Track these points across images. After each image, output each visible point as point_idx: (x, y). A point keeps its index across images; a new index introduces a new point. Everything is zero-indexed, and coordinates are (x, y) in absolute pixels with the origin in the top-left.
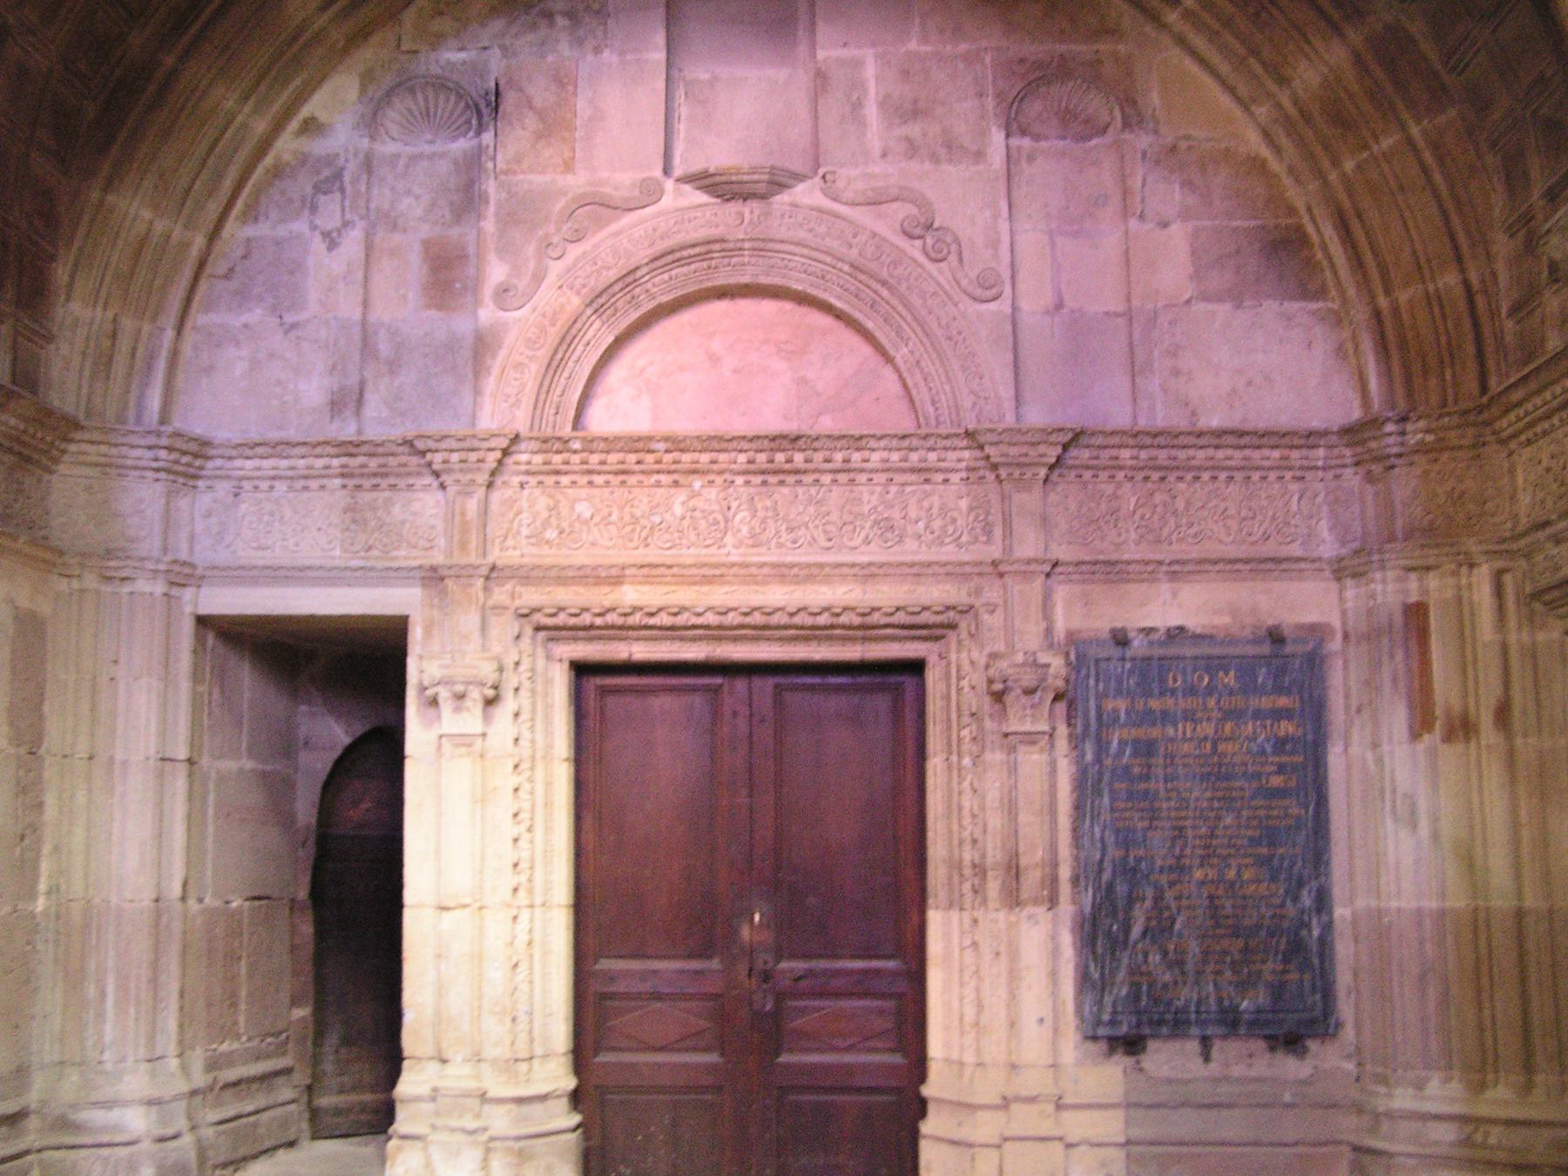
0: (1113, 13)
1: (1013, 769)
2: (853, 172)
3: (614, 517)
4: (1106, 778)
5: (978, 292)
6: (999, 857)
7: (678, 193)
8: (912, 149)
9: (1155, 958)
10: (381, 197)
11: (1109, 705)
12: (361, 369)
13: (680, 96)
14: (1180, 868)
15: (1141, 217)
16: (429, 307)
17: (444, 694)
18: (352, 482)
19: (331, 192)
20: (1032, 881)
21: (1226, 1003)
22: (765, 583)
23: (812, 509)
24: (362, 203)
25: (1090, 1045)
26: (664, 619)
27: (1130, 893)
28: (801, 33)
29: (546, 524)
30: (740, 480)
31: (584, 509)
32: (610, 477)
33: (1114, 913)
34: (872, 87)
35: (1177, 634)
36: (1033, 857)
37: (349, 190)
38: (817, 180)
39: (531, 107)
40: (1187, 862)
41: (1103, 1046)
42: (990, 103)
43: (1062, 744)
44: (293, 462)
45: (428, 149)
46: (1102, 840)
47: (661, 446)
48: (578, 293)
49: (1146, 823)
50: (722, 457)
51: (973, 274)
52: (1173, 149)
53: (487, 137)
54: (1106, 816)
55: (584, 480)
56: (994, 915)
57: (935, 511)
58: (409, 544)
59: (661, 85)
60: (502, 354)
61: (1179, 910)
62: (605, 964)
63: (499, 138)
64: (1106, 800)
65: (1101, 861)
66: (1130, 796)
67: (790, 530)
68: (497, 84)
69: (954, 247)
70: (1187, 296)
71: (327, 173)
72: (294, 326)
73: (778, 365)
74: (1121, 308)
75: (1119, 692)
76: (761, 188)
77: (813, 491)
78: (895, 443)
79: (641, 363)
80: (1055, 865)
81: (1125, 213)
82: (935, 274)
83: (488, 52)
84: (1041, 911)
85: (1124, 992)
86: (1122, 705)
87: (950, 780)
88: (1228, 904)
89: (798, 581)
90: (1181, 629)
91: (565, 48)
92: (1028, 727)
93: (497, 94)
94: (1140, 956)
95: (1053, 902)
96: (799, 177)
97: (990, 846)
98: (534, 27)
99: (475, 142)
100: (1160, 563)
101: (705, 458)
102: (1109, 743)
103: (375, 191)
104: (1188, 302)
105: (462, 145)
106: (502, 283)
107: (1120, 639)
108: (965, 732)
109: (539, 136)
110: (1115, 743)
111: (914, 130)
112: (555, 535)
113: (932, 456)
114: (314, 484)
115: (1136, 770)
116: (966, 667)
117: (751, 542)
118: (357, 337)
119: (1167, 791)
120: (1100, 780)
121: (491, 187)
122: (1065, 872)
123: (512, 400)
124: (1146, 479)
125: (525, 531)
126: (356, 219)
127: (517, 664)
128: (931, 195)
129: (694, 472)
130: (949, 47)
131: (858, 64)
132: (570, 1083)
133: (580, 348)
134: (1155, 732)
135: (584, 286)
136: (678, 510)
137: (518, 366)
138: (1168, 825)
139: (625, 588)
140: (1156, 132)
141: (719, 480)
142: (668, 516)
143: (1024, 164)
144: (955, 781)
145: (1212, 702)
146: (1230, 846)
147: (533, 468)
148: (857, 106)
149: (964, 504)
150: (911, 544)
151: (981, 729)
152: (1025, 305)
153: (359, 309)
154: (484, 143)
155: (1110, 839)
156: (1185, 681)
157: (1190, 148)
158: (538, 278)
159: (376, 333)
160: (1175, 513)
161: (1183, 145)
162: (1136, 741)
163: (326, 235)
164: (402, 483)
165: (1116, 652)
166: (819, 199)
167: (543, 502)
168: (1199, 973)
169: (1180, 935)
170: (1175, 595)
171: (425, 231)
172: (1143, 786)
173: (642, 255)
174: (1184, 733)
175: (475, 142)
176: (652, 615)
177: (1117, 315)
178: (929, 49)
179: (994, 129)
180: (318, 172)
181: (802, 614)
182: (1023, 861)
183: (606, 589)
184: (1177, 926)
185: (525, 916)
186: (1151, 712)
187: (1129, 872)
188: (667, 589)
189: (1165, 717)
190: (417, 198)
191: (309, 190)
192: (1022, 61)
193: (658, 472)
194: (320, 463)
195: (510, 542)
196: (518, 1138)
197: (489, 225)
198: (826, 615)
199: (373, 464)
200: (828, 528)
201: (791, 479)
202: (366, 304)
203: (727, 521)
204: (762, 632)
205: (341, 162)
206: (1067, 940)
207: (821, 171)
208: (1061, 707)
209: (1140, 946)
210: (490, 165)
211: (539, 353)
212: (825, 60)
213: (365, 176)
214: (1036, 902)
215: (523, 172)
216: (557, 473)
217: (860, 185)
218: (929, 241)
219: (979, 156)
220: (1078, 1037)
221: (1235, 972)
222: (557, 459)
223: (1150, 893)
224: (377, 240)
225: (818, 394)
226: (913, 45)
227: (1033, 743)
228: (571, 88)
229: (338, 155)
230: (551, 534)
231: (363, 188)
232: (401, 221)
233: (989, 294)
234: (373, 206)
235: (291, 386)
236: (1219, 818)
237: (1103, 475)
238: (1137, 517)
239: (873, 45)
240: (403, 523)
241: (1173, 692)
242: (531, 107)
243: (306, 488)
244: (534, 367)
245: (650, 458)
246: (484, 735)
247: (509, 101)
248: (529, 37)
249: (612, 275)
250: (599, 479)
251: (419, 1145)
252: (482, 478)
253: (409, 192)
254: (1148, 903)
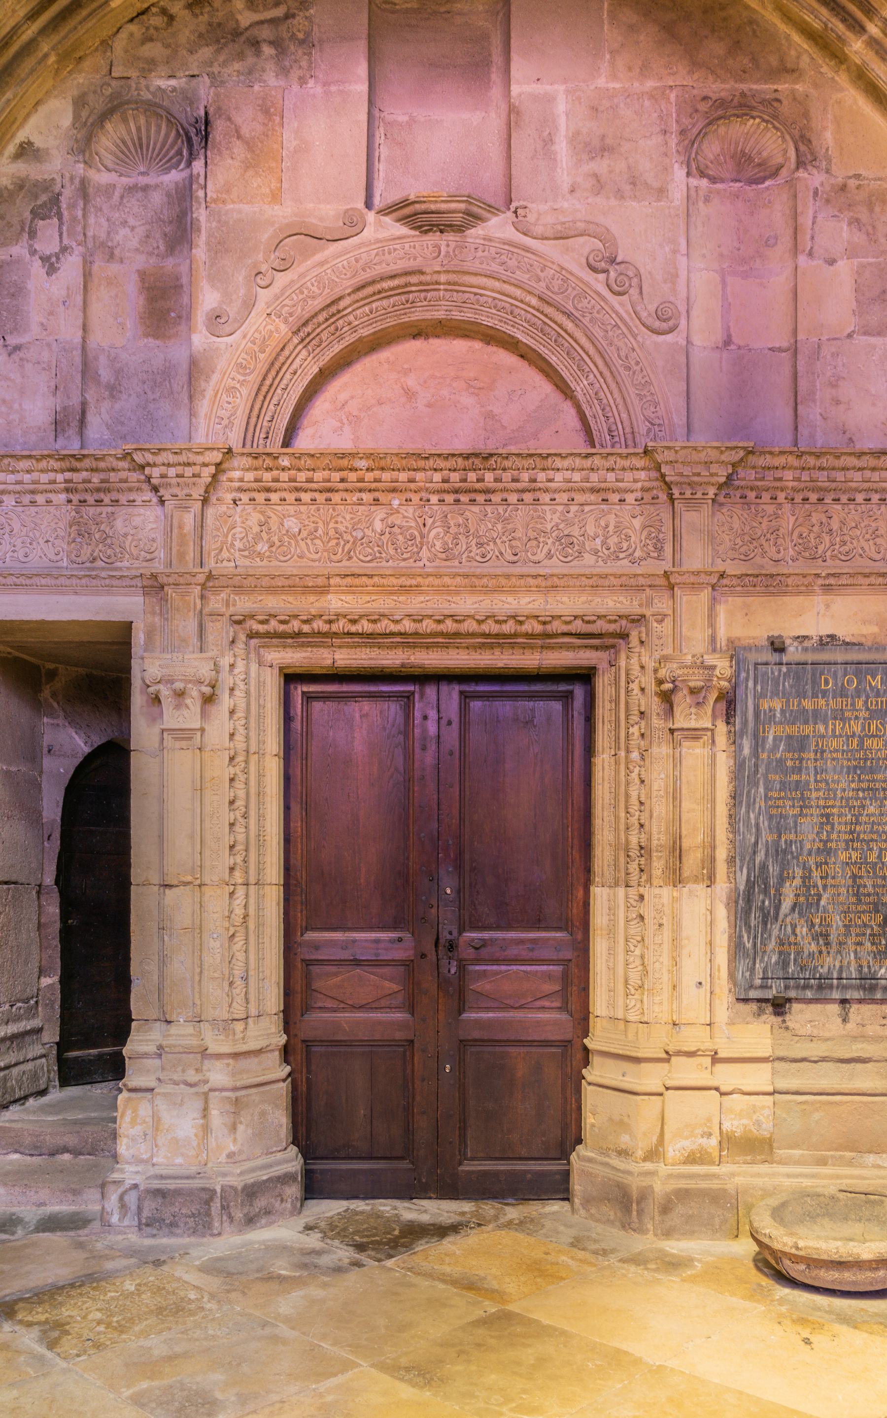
0: (793, 53)
1: (677, 762)
2: (543, 207)
3: (320, 532)
4: (762, 770)
5: (657, 324)
6: (663, 837)
7: (380, 225)
8: (599, 185)
9: (802, 930)
10: (97, 226)
11: (765, 705)
12: (83, 391)
13: (380, 134)
14: (827, 851)
15: (810, 254)
16: (147, 335)
17: (165, 692)
18: (75, 498)
19: (50, 218)
20: (692, 862)
21: (866, 970)
22: (457, 593)
23: (499, 526)
24: (79, 228)
25: (741, 1006)
26: (365, 626)
27: (782, 872)
28: (495, 76)
29: (258, 538)
30: (434, 499)
31: (292, 524)
32: (317, 495)
33: (766, 891)
34: (562, 121)
35: (829, 641)
36: (693, 840)
37: (66, 214)
38: (510, 214)
39: (239, 137)
40: (833, 845)
42: (673, 141)
43: (722, 740)
44: (18, 476)
45: (143, 180)
46: (757, 825)
47: (363, 464)
48: (286, 321)
49: (797, 811)
50: (419, 476)
51: (652, 308)
52: (844, 188)
53: (198, 166)
54: (760, 803)
55: (291, 497)
56: (657, 891)
57: (611, 528)
58: (131, 554)
59: (364, 117)
60: (215, 377)
61: (825, 887)
62: (312, 936)
63: (209, 168)
64: (761, 790)
65: (757, 843)
66: (783, 786)
67: (480, 545)
68: (206, 114)
69: (635, 281)
70: (849, 330)
71: (44, 198)
72: (17, 348)
73: (467, 400)
74: (785, 344)
75: (775, 694)
76: (457, 218)
77: (501, 509)
78: (578, 462)
79: (343, 397)
80: (713, 848)
81: (795, 250)
82: (617, 307)
83: (195, 80)
84: (700, 889)
85: (774, 959)
86: (778, 705)
87: (617, 772)
88: (869, 883)
89: (488, 591)
90: (832, 637)
91: (272, 79)
92: (693, 724)
93: (207, 123)
94: (789, 929)
95: (711, 880)
96: (493, 209)
97: (655, 830)
98: (241, 56)
99: (185, 174)
100: (817, 576)
101: (403, 476)
102: (765, 739)
103: (92, 220)
104: (850, 336)
105: (175, 176)
106: (213, 309)
107: (777, 646)
108: (634, 730)
109: (248, 166)
110: (771, 738)
111: (601, 166)
112: (266, 548)
113: (611, 476)
114: (40, 499)
115: (789, 763)
116: (636, 670)
117: (443, 556)
118: (78, 360)
119: (816, 781)
120: (756, 772)
121: (201, 214)
122: (722, 854)
123: (225, 422)
124: (806, 499)
125: (238, 544)
126: (74, 244)
127: (232, 666)
128: (614, 229)
129: (394, 490)
130: (636, 84)
131: (550, 99)
132: (284, 1039)
133: (288, 376)
134: (808, 730)
135: (291, 315)
136: (378, 526)
137: (231, 390)
138: (815, 812)
139: (330, 597)
140: (828, 171)
141: (415, 498)
142: (369, 532)
143: (701, 204)
144: (623, 773)
145: (860, 704)
146: (872, 832)
147: (245, 485)
148: (549, 141)
149: (637, 523)
150: (589, 559)
151: (649, 726)
152: (697, 340)
153: (80, 333)
154: (195, 172)
155: (764, 824)
156: (835, 684)
157: (858, 187)
158: (249, 304)
159: (96, 359)
161: (852, 183)
162: (790, 737)
163: (45, 259)
164: (123, 499)
165: (775, 657)
166: (510, 233)
167: (255, 518)
169: (825, 910)
170: (828, 606)
171: (140, 261)
172: (795, 777)
173: (348, 284)
174: (834, 730)
175: (188, 171)
176: (354, 622)
177: (781, 350)
178: (617, 85)
179: (676, 166)
180: (36, 197)
181: (489, 621)
182: (686, 844)
183: (312, 598)
184: (822, 903)
185: (241, 892)
186: (804, 711)
187: (780, 853)
188: (368, 598)
189: (817, 716)
190: (133, 228)
191: (27, 215)
192: (705, 98)
193: (360, 491)
194: (45, 478)
195: (225, 554)
196: (235, 1089)
197: (200, 252)
198: (511, 622)
199: (96, 479)
200: (514, 543)
201: (481, 498)
202: (85, 328)
203: (422, 536)
204: (451, 640)
205: (57, 188)
206: (722, 913)
207: (513, 207)
208: (722, 706)
209: (788, 919)
210: (201, 194)
211: (249, 378)
212: (520, 95)
213: (81, 203)
214: (696, 880)
215: (233, 202)
216: (268, 490)
217: (550, 219)
218: (613, 274)
219: (662, 192)
220: (732, 999)
221: (873, 944)
222: (267, 476)
223: (799, 872)
224: (96, 267)
225: (504, 428)
226: (601, 82)
227: (697, 738)
228: (277, 119)
229: (53, 179)
230: (262, 547)
231: (80, 213)
232: (117, 252)
233: (665, 326)
234: (90, 234)
235: (16, 406)
236: (863, 807)
238: (796, 534)
239: (565, 81)
240: (125, 535)
241: (825, 693)
242: (239, 137)
243: (33, 503)
244: (245, 391)
245: (353, 476)
246: (202, 730)
247: (219, 127)
248: (237, 66)
249: (318, 303)
250: (306, 497)
251: (148, 1095)
252: (197, 492)
253: (124, 223)
254: (797, 882)
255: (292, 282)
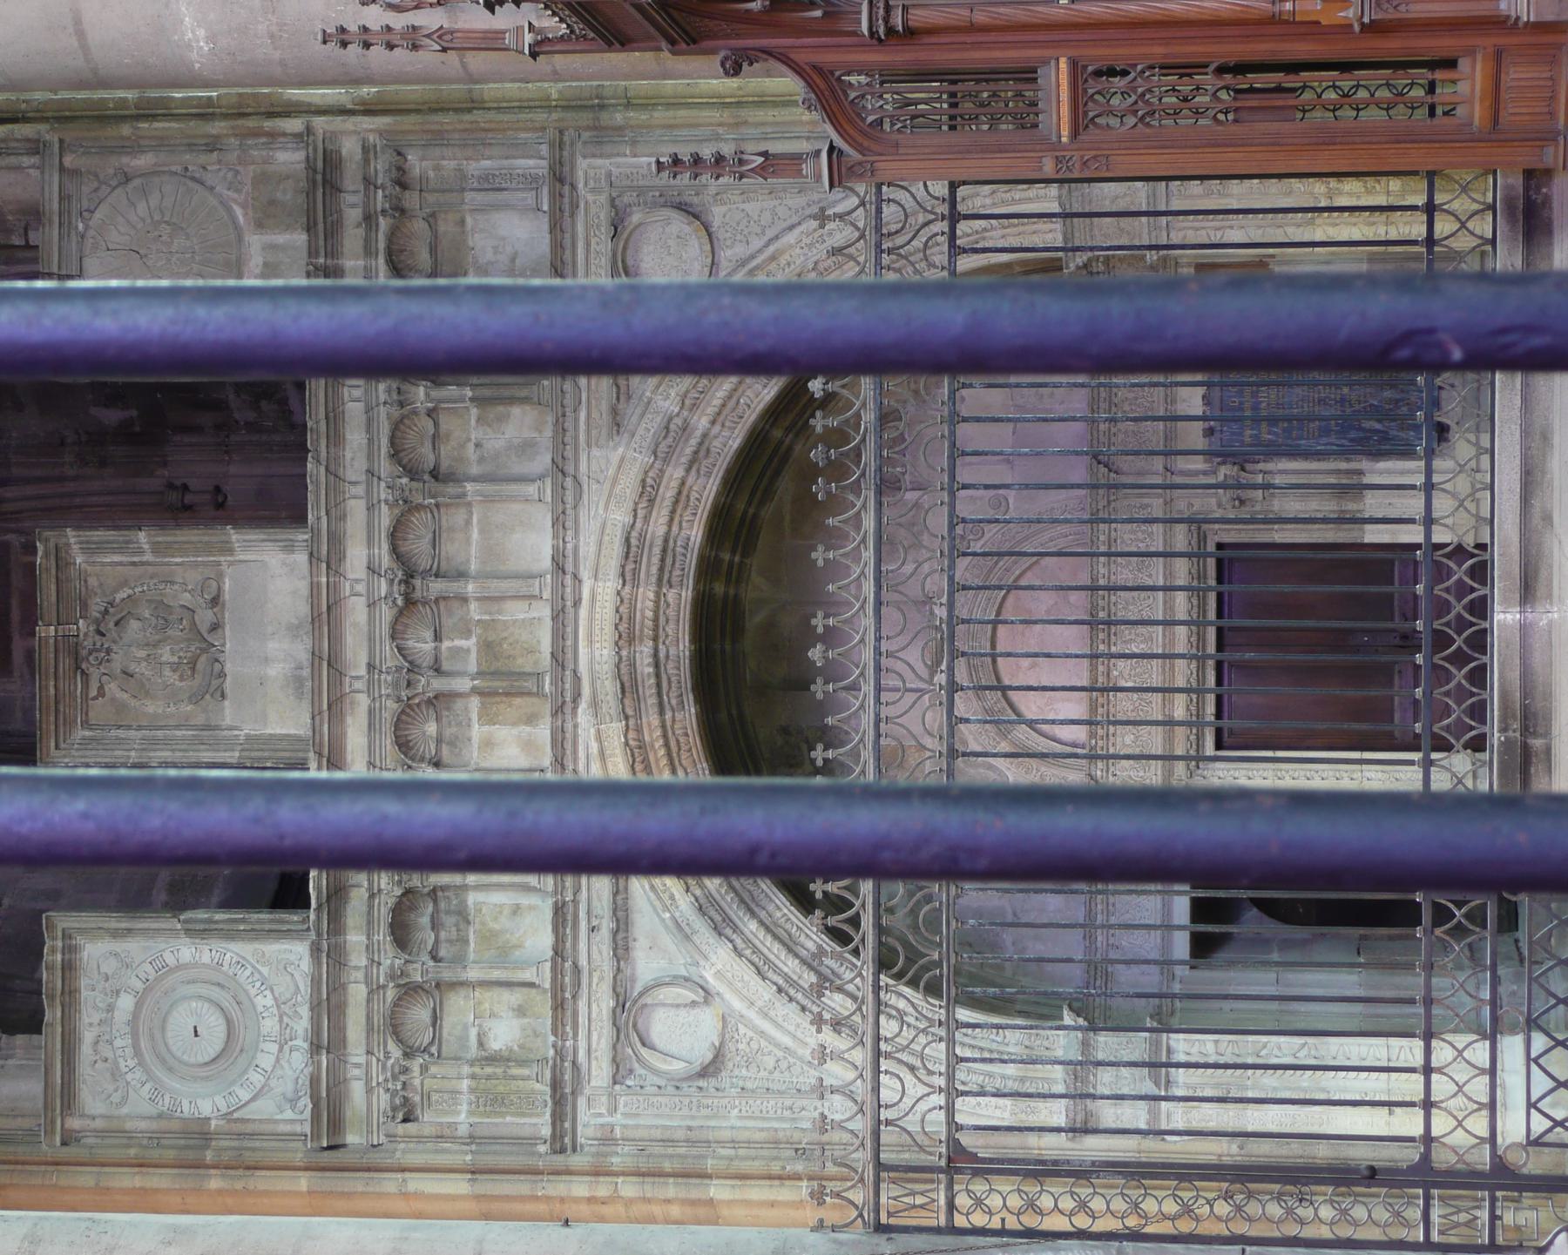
4: (1289, 442)
11: (1248, 440)
14: (1343, 401)
33: (1368, 439)
40: (1338, 397)
41: (1444, 445)
44: (1099, 911)
48: (998, 743)
64: (1303, 442)
75: (1241, 434)
90: (1204, 397)
102: (1269, 440)
113: (1102, 538)
125: (1141, 774)
129: (1108, 675)
138: (1316, 409)
155: (1324, 440)
160: (1136, 399)
165: (1217, 435)
168: (1402, 391)
169: (1380, 401)
208: (1249, 466)
218: (971, 537)
225: (1056, 603)
237: (1113, 439)
241: (1241, 403)
243: (1114, 905)
244: (1043, 769)
255: (975, 739)
